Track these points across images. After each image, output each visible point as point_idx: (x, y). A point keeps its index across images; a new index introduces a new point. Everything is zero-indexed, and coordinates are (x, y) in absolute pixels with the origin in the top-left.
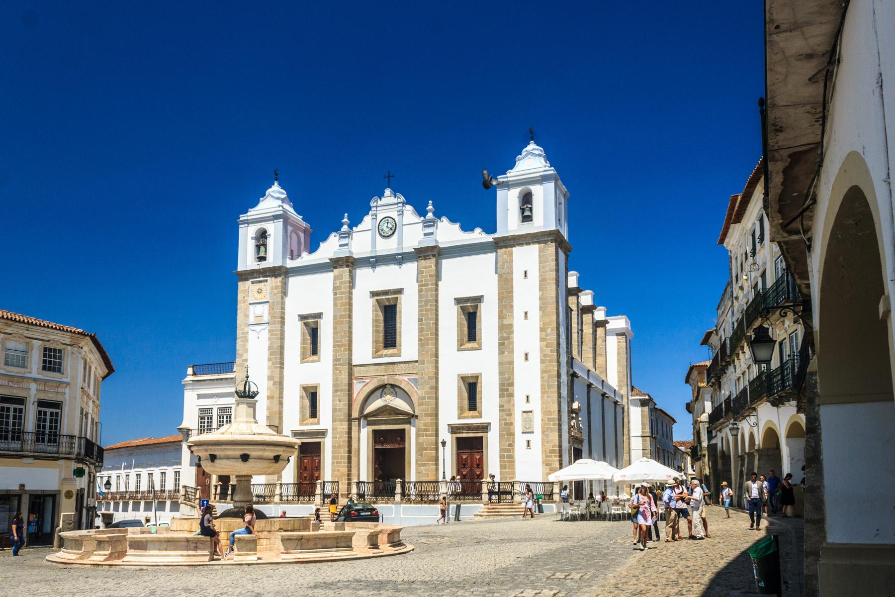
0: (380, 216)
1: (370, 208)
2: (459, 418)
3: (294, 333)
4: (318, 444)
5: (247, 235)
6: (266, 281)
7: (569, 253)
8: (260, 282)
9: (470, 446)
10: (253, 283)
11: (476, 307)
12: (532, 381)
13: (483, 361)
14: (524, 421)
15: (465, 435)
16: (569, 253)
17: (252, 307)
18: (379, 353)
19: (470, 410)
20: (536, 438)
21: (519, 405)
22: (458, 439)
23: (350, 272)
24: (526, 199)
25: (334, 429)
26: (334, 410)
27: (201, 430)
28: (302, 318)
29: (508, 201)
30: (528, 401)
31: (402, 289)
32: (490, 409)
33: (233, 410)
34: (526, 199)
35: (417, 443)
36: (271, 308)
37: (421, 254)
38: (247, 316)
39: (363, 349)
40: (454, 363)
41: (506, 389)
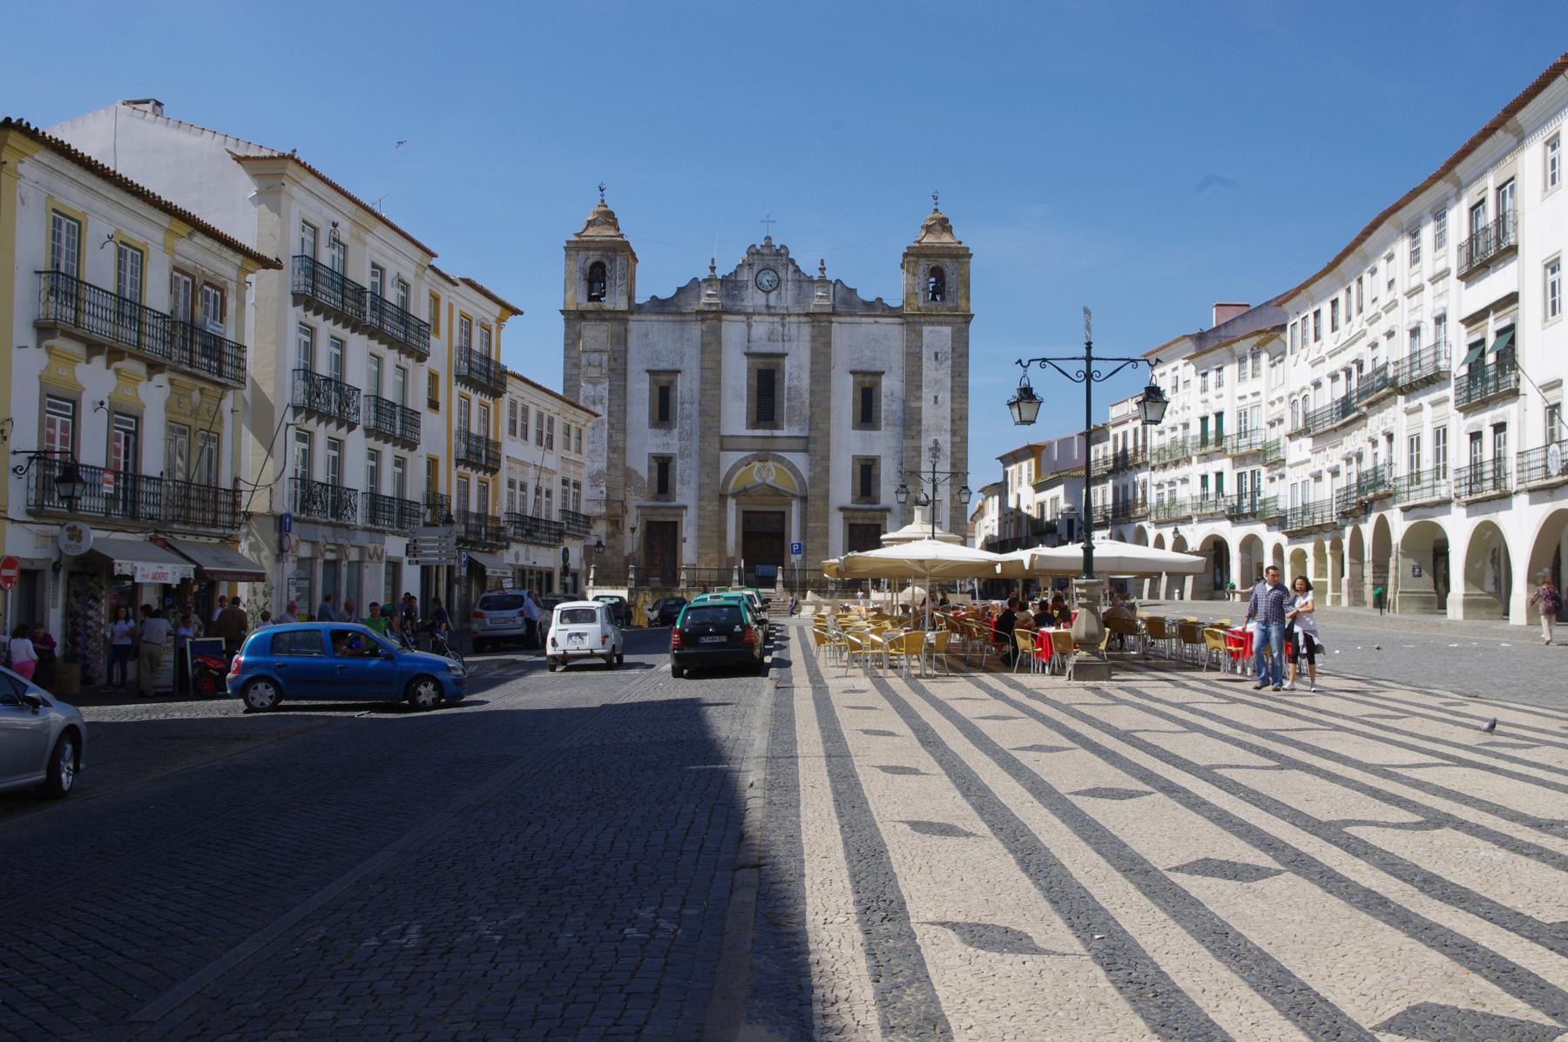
3: (640, 391)
4: (675, 523)
11: (878, 384)
25: (700, 508)
26: (701, 486)
28: (651, 372)
40: (848, 443)
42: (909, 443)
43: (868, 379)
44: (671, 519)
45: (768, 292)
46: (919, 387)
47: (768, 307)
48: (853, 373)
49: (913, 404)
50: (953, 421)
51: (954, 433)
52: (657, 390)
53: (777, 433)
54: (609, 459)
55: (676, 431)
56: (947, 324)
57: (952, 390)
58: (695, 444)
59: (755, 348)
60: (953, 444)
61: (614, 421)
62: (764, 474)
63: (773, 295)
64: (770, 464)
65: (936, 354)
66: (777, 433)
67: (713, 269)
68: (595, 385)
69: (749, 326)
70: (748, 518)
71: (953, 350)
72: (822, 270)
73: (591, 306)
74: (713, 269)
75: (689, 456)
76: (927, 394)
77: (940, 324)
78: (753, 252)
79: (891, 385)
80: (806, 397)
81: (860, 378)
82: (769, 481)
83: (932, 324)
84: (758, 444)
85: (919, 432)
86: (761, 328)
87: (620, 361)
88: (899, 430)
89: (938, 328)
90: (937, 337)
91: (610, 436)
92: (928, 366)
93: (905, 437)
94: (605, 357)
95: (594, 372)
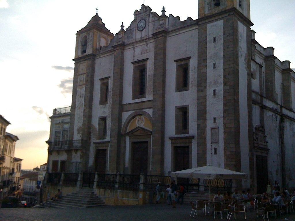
6: (85, 62)
8: (83, 63)
12: (215, 108)
14: (212, 135)
15: (178, 145)
17: (79, 77)
21: (210, 124)
22: (174, 146)
30: (215, 122)
31: (148, 59)
36: (87, 76)
40: (174, 99)
43: (183, 63)
44: (104, 148)
45: (141, 31)
46: (205, 60)
47: (141, 38)
48: (176, 61)
50: (224, 77)
51: (225, 84)
52: (105, 87)
53: (144, 99)
55: (108, 105)
56: (220, 19)
60: (225, 91)
62: (140, 121)
63: (143, 31)
64: (142, 117)
65: (215, 38)
66: (144, 99)
67: (122, 26)
68: (81, 89)
69: (134, 49)
70: (134, 144)
71: (224, 34)
72: (164, 11)
74: (122, 26)
76: (210, 63)
78: (136, 13)
79: (193, 64)
81: (180, 63)
82: (142, 126)
83: (212, 21)
86: (138, 50)
87: (89, 77)
89: (215, 23)
91: (84, 110)
93: (198, 91)
95: (81, 83)
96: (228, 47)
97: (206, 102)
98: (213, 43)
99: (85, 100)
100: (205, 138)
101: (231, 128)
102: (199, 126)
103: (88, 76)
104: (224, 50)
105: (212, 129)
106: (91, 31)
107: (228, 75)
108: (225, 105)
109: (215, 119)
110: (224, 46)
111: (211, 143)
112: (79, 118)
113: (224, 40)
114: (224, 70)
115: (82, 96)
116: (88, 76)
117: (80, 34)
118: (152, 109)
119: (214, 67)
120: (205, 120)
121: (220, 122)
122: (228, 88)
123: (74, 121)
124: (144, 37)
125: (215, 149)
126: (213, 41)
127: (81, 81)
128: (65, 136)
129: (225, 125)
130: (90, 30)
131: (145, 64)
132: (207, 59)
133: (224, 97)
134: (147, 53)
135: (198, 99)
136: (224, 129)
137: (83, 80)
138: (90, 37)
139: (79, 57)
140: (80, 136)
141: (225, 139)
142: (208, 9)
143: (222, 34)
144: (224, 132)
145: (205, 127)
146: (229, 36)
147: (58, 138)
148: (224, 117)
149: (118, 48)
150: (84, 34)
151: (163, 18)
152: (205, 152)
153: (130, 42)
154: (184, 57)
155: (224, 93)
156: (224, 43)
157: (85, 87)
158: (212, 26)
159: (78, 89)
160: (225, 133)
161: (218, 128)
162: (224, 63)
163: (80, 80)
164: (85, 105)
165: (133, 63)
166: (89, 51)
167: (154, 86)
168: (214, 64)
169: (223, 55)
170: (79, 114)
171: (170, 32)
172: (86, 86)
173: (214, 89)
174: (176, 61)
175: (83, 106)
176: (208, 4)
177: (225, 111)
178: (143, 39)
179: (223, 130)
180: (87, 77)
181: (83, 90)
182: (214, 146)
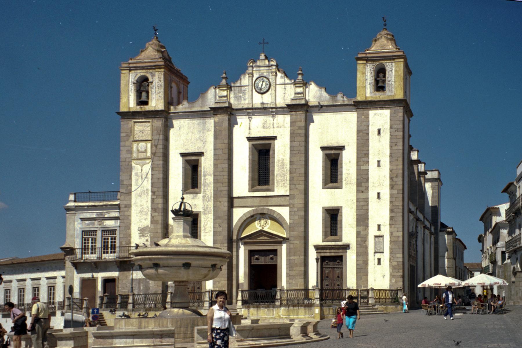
0: (256, 76)
1: (247, 68)
2: (323, 242)
5: (129, 81)
6: (149, 122)
7: (411, 118)
9: (332, 261)
10: (135, 122)
13: (344, 198)
14: (375, 243)
15: (328, 254)
16: (411, 118)
17: (135, 145)
18: (254, 188)
19: (332, 235)
20: (386, 257)
21: (372, 231)
23: (229, 120)
24: (380, 74)
27: (84, 250)
28: (183, 155)
29: (366, 75)
32: (349, 233)
33: (117, 233)
34: (380, 74)
35: (289, 261)
37: (291, 108)
38: (130, 151)
39: (241, 185)
41: (362, 219)
42: (362, 196)
46: (367, 155)
49: (363, 168)
50: (391, 178)
51: (392, 187)
54: (152, 217)
57: (391, 156)
58: (211, 204)
59: (253, 135)
60: (392, 195)
61: (155, 190)
71: (391, 127)
73: (138, 108)
75: (209, 212)
77: (382, 108)
80: (288, 166)
83: (376, 109)
84: (257, 202)
85: (367, 188)
87: (160, 146)
88: (355, 187)
90: (380, 119)
91: (153, 201)
92: (374, 141)
93: (358, 191)
94: (149, 145)
95: (141, 156)
96: (396, 145)
97: (368, 205)
98: (378, 137)
99: (152, 183)
100: (366, 248)
101: (398, 236)
102: (358, 234)
103: (156, 146)
104: (391, 147)
105: (376, 237)
106: (158, 70)
107: (396, 177)
108: (392, 211)
109: (379, 226)
110: (391, 142)
111: (375, 253)
112: (141, 212)
113: (390, 135)
114: (391, 170)
115: (144, 176)
116: (156, 146)
117: (130, 70)
118: (288, 208)
119: (379, 166)
120: (367, 226)
121: (386, 231)
122: (395, 192)
123: (130, 216)
124: (267, 104)
125: (379, 260)
126: (377, 133)
127: (142, 152)
128: (108, 239)
129: (391, 233)
130: (155, 69)
131: (270, 144)
132: (368, 154)
133: (391, 202)
134: (274, 127)
135: (358, 200)
136: (390, 238)
137: (146, 151)
138: (157, 80)
139: (131, 110)
140: (147, 241)
141: (391, 249)
142: (370, 90)
143: (388, 127)
144: (390, 241)
145: (367, 235)
146: (397, 131)
147: (90, 241)
148: (390, 225)
149: (220, 111)
150: (139, 71)
151: (302, 85)
152: (366, 263)
153: (240, 107)
154: (335, 145)
155: (390, 197)
156: (391, 139)
157: (151, 163)
158: (375, 114)
159: (133, 165)
160: (391, 242)
161: (382, 236)
162: (390, 162)
163: (138, 150)
164: (153, 193)
165: (249, 139)
166: (156, 102)
167: (291, 179)
168: (379, 162)
169: (391, 153)
170: (141, 206)
171: (312, 107)
172: (152, 162)
173: (378, 191)
174: (323, 148)
175: (150, 193)
176: (370, 84)
177: (391, 218)
178: (266, 106)
179: (389, 239)
180: (154, 146)
181: (147, 167)
182: (378, 256)
